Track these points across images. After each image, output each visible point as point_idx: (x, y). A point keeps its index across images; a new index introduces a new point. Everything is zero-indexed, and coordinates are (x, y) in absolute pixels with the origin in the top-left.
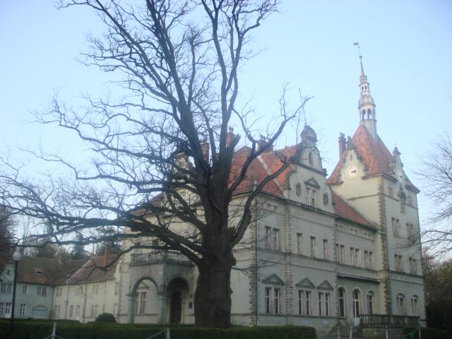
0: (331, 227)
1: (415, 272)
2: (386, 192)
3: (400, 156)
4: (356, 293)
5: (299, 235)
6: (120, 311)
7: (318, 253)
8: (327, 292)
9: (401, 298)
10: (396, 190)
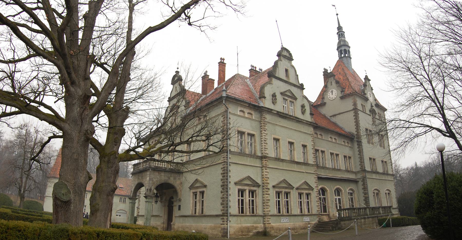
0: (310, 134)
1: (387, 171)
2: (360, 107)
4: (338, 192)
5: (277, 140)
7: (299, 157)
8: (307, 192)
9: (377, 193)
10: (368, 107)
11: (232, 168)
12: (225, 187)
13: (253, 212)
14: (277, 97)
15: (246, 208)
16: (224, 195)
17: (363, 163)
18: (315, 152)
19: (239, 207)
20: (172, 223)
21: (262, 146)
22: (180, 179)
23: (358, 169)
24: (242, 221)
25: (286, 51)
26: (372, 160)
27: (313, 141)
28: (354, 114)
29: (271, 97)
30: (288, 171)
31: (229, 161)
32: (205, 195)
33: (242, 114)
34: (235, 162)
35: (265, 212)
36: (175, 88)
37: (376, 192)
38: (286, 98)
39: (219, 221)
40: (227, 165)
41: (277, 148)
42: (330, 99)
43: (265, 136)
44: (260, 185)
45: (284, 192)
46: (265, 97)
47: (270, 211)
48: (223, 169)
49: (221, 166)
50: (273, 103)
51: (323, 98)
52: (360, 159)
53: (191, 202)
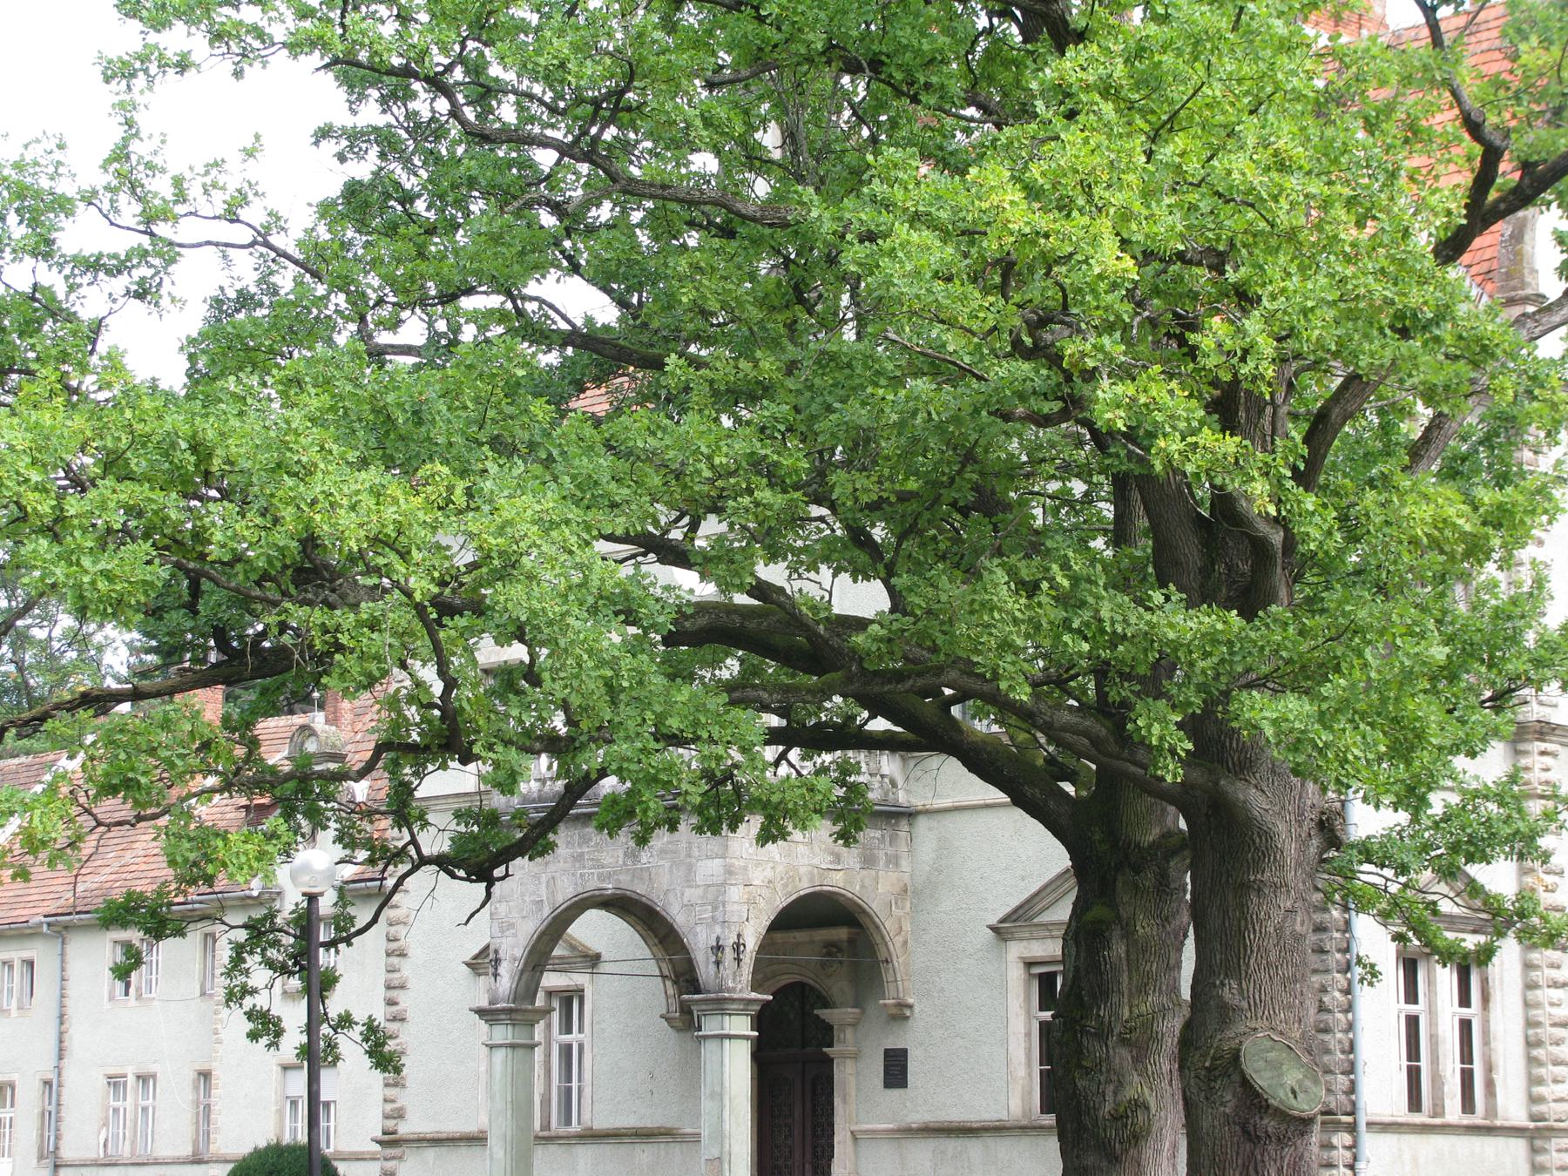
6: (399, 1115)
22: (894, 861)
35: (1537, 1109)
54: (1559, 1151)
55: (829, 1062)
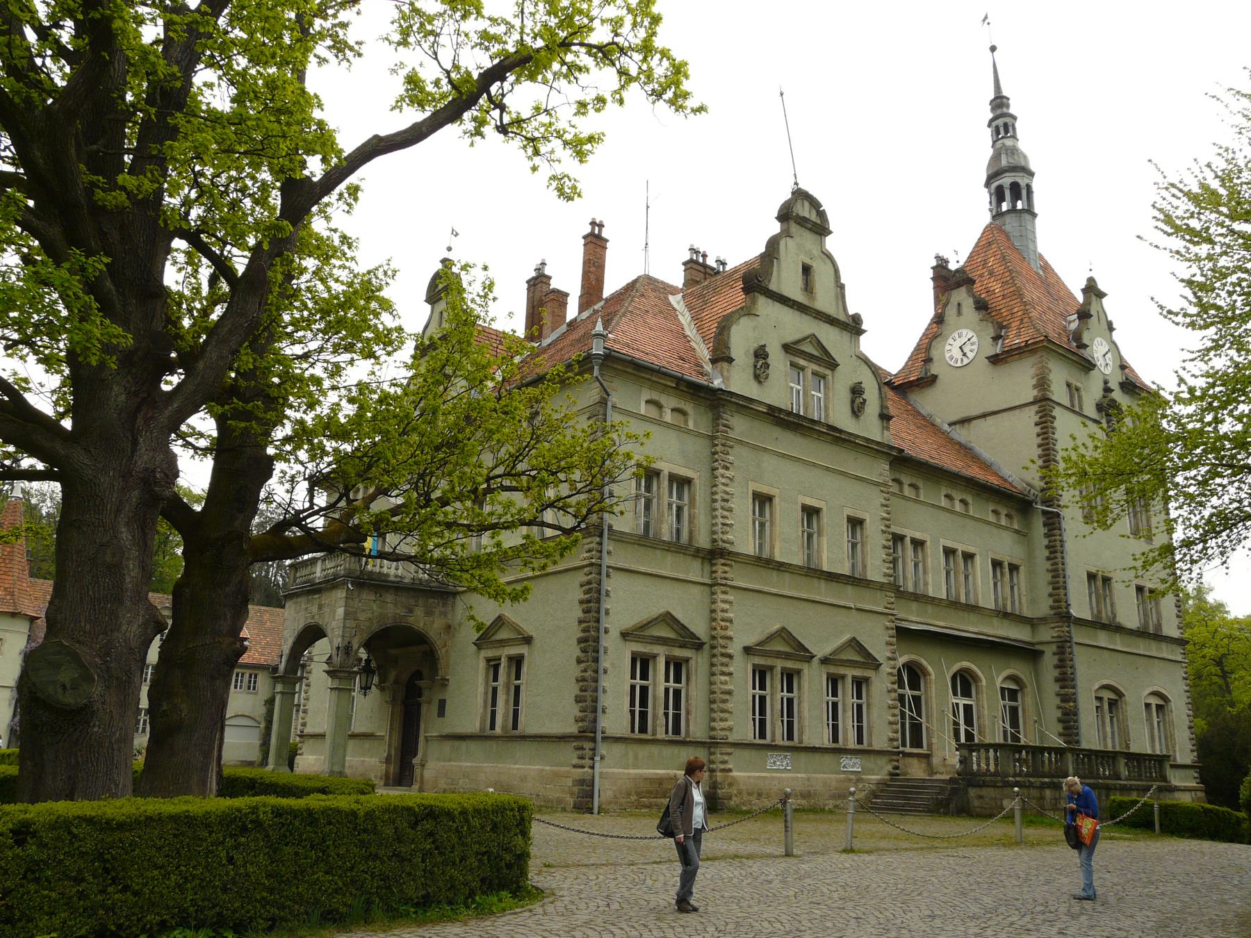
0: (877, 484)
1: (1159, 626)
2: (1059, 393)
3: (1104, 300)
5: (763, 500)
8: (858, 673)
9: (1113, 701)
10: (1092, 394)
11: (614, 584)
12: (590, 645)
13: (677, 730)
14: (769, 361)
15: (655, 717)
16: (585, 671)
17: (1062, 592)
18: (891, 543)
19: (632, 713)
20: (414, 761)
21: (716, 517)
23: (1043, 608)
24: (640, 757)
25: (807, 204)
26: (1099, 581)
27: (886, 506)
28: (1036, 418)
29: (752, 360)
30: (795, 602)
31: (607, 561)
32: (525, 669)
33: (653, 412)
34: (626, 566)
36: (436, 315)
37: (1107, 695)
38: (802, 362)
39: (569, 754)
40: (600, 574)
41: (762, 525)
42: (952, 363)
43: (727, 485)
44: (704, 644)
45: (779, 669)
46: (730, 360)
47: (730, 729)
48: (587, 587)
49: (581, 577)
50: (757, 377)
51: (928, 360)
52: (1053, 577)
53: (481, 689)
54: (721, 754)
55: (419, 705)
